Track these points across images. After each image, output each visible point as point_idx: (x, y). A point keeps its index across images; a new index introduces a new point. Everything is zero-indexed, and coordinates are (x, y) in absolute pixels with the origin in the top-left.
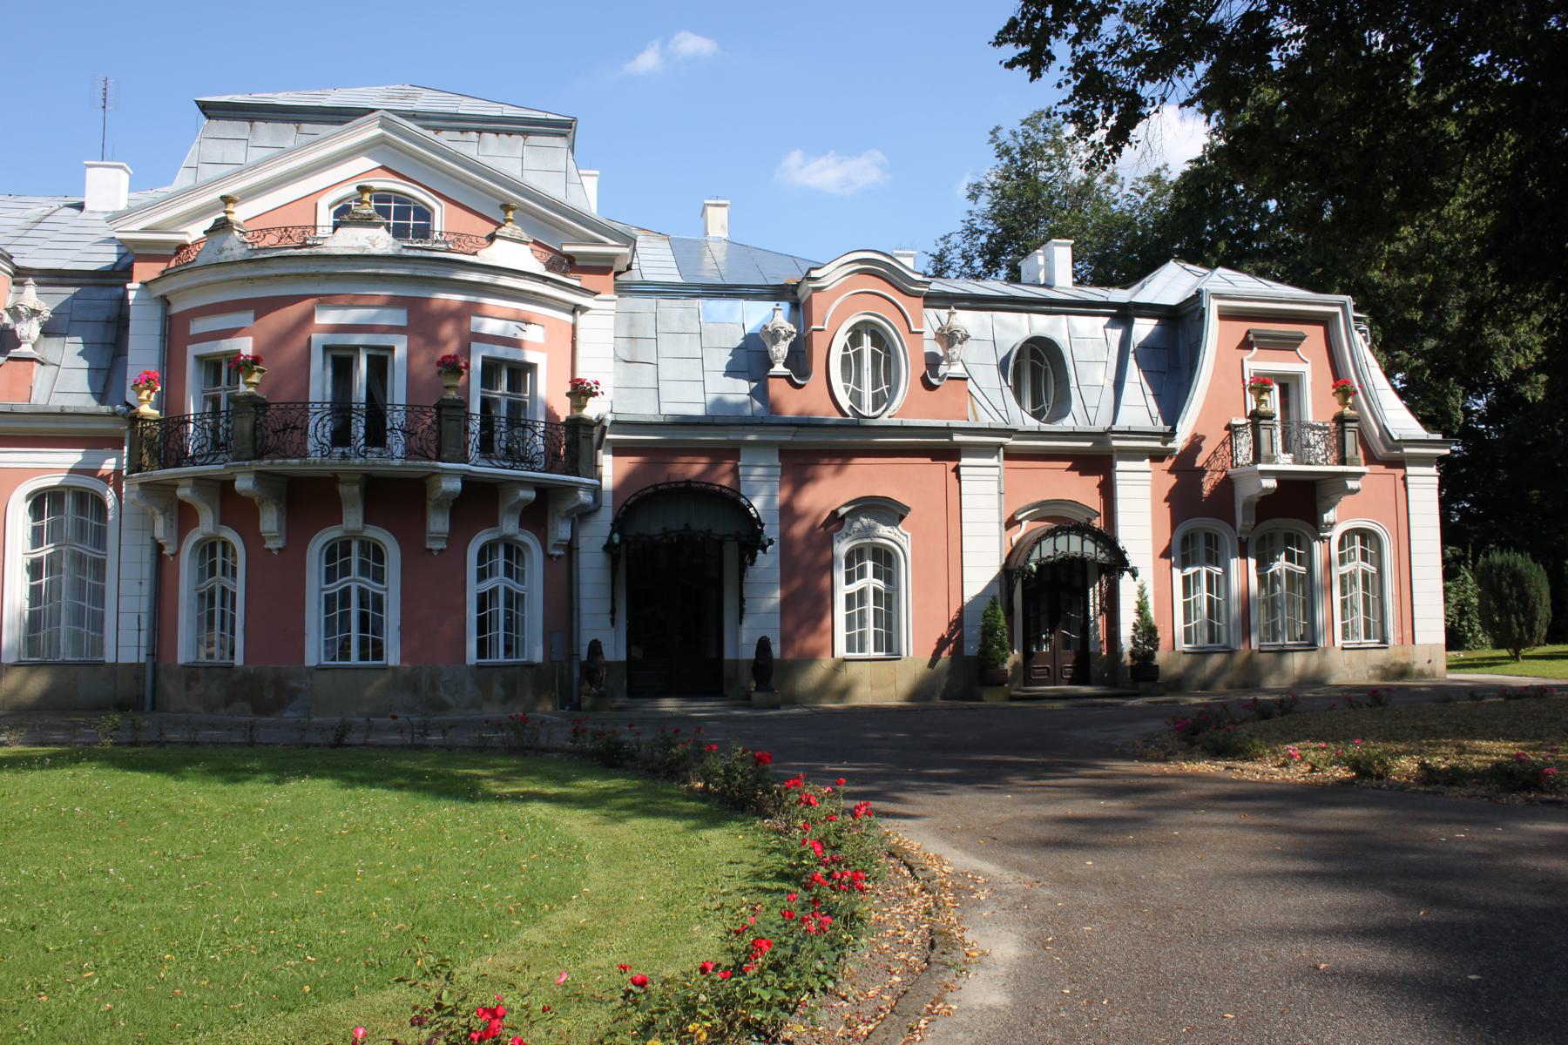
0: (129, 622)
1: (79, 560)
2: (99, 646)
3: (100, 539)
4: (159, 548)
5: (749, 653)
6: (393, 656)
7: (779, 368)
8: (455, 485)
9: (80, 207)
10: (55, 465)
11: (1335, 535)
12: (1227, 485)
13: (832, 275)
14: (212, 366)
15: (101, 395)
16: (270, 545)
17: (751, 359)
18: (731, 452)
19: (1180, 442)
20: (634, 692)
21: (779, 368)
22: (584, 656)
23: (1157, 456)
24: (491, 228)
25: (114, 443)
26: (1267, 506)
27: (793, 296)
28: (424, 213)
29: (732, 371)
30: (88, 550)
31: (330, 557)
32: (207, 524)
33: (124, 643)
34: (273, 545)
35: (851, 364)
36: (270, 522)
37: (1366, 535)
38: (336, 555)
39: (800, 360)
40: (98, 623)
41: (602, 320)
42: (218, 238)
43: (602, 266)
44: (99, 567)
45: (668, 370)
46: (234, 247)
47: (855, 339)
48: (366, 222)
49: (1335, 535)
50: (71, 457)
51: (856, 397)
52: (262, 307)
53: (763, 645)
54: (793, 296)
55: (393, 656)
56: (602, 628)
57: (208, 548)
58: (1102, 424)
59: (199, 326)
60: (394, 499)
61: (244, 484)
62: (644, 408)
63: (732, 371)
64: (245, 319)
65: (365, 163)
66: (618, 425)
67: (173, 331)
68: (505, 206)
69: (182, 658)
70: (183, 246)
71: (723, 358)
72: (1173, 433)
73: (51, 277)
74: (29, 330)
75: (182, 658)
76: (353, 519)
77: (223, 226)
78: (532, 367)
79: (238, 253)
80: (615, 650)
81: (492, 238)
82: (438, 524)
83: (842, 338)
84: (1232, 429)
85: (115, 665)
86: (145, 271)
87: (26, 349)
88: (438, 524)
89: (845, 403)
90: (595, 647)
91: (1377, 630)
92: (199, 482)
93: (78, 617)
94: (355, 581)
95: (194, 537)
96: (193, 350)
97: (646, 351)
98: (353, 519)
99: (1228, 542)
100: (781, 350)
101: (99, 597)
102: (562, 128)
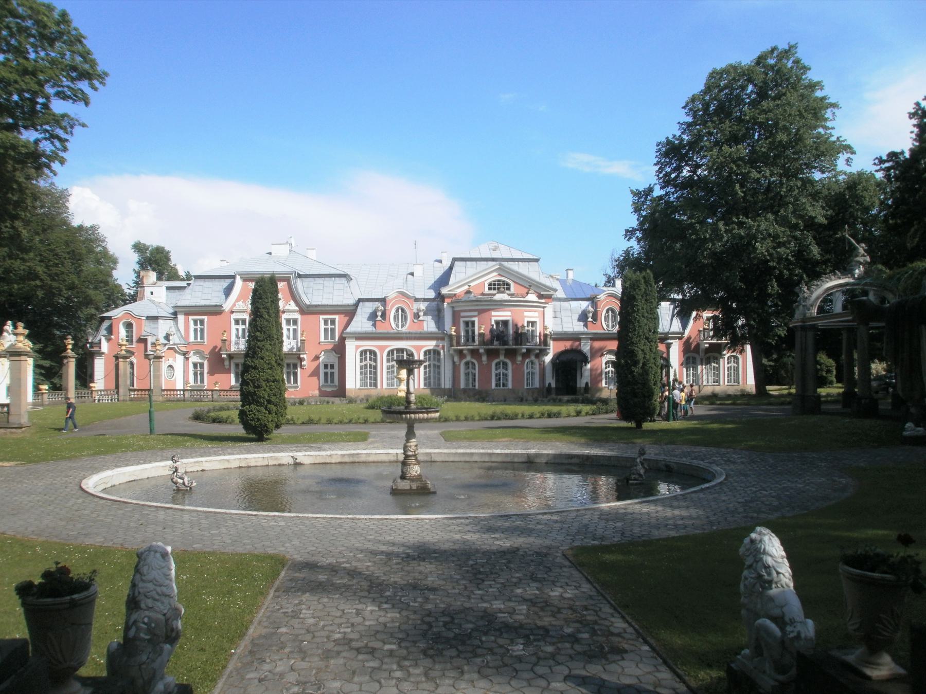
0: (447, 379)
1: (434, 365)
2: (439, 384)
3: (439, 360)
4: (454, 363)
5: (583, 385)
6: (510, 386)
7: (590, 319)
8: (524, 351)
9: (412, 274)
10: (431, 344)
11: (726, 357)
12: (698, 345)
13: (602, 297)
14: (467, 323)
15: (438, 328)
16: (485, 363)
17: (583, 317)
18: (579, 340)
19: (686, 335)
20: (557, 394)
21: (590, 319)
22: (547, 385)
23: (680, 338)
24: (526, 290)
25: (443, 339)
26: (707, 350)
27: (593, 300)
28: (508, 285)
29: (579, 320)
30: (437, 363)
31: (496, 365)
32: (468, 358)
33: (447, 383)
34: (485, 363)
35: (606, 318)
36: (484, 358)
37: (735, 357)
38: (497, 364)
39: (595, 317)
40: (439, 379)
41: (549, 309)
42: (468, 295)
43: (549, 297)
44: (439, 367)
45: (564, 319)
46: (472, 297)
47: (607, 311)
48: (503, 292)
49: (726, 357)
50: (434, 343)
51: (608, 326)
52: (481, 312)
53: (587, 384)
54: (593, 300)
55: (510, 386)
56: (550, 380)
57: (467, 364)
58: (667, 330)
59: (462, 314)
60: (511, 354)
61: (481, 351)
62: (559, 329)
63: (579, 320)
64: (476, 313)
65: (495, 274)
66: (555, 334)
67: (456, 316)
68: (530, 285)
69: (462, 386)
70: (455, 295)
71: (576, 317)
72: (683, 333)
73: (425, 300)
74: (421, 314)
75: (462, 386)
76: (502, 358)
77: (468, 292)
78: (535, 322)
79: (474, 299)
80: (553, 385)
81: (527, 293)
82: (519, 358)
83: (604, 312)
84: (699, 331)
85: (445, 389)
86: (447, 301)
87: (421, 318)
88: (519, 358)
89: (605, 327)
90: (550, 384)
91: (737, 380)
92: (468, 350)
93: (434, 378)
94: (501, 371)
95: (464, 361)
96: (462, 320)
97: (558, 315)
98: (502, 358)
99: (698, 360)
100: (591, 315)
101: (439, 373)
102: (537, 260)
